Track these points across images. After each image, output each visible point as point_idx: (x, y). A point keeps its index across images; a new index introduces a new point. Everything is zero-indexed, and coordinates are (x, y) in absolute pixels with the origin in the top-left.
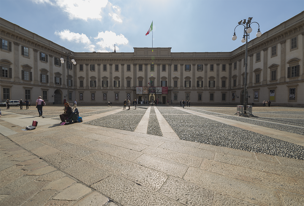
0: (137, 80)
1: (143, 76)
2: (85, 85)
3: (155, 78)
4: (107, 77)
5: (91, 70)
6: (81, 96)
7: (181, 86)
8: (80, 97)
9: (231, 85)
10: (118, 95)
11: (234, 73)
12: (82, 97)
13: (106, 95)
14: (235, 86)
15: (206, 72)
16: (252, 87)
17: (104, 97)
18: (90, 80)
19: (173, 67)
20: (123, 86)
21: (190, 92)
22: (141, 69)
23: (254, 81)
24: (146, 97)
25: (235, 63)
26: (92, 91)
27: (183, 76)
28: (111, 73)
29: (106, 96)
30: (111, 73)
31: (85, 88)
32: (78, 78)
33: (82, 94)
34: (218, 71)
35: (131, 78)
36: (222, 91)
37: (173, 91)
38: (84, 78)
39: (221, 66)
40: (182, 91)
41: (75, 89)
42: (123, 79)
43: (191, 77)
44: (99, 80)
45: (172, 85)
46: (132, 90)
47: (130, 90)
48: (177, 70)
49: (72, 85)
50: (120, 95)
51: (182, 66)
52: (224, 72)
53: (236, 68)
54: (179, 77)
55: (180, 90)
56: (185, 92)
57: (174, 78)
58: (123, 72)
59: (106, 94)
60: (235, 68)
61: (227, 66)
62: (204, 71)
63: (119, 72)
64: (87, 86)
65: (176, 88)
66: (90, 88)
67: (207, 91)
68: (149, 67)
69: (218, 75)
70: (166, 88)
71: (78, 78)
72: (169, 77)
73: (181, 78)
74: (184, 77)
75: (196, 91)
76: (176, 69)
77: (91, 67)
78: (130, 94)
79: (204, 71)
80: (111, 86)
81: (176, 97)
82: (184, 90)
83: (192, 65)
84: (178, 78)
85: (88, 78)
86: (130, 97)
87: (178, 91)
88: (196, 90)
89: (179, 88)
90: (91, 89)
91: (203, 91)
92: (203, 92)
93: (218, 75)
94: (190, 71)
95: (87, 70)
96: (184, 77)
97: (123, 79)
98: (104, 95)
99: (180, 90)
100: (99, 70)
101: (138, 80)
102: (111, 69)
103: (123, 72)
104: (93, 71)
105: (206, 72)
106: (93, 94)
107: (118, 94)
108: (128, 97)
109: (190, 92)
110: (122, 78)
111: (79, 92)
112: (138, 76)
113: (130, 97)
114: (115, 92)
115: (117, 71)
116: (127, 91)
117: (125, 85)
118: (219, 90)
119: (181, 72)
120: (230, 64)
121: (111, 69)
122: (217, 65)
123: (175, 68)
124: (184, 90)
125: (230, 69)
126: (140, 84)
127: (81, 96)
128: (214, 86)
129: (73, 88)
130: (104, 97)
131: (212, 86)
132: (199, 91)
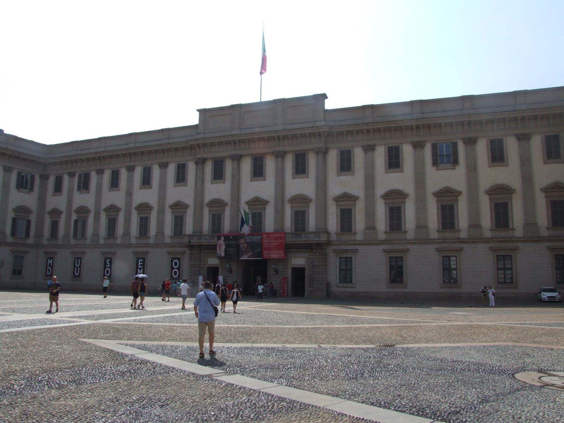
0: (206, 211)
2: (61, 232)
3: (267, 202)
5: (79, 189)
6: (50, 264)
7: (367, 228)
8: (47, 266)
10: (144, 262)
12: (52, 267)
15: (472, 169)
17: (105, 268)
18: (74, 217)
19: (333, 158)
21: (407, 251)
22: (218, 175)
24: (231, 271)
28: (129, 194)
29: (110, 267)
30: (129, 194)
31: (60, 242)
32: (49, 213)
33: (52, 258)
35: (186, 207)
36: (552, 244)
37: (335, 248)
41: (36, 246)
42: (161, 212)
45: (333, 224)
46: (191, 247)
49: (27, 235)
55: (363, 243)
56: (385, 251)
57: (339, 199)
59: (111, 259)
62: (461, 168)
64: (67, 235)
66: (73, 242)
67: (481, 245)
68: (247, 166)
70: (277, 238)
71: (49, 213)
73: (366, 196)
74: (380, 190)
78: (179, 259)
79: (461, 168)
82: (382, 242)
84: (354, 199)
86: (179, 268)
87: (357, 247)
88: (431, 241)
89: (359, 237)
91: (465, 246)
92: (461, 250)
95: (71, 191)
96: (380, 190)
97: (161, 212)
98: (105, 264)
99: (363, 243)
100: (99, 186)
101: (210, 211)
104: (84, 190)
105: (472, 169)
106: (78, 258)
107: (144, 259)
108: (172, 268)
109: (407, 251)
110: (159, 206)
111: (46, 253)
112: (207, 199)
113: (179, 268)
114: (135, 253)
115: (147, 186)
116: (171, 249)
117: (168, 230)
118: (537, 239)
121: (130, 181)
124: (382, 242)
127: (50, 264)
129: (30, 241)
130: (105, 268)
132: (445, 245)
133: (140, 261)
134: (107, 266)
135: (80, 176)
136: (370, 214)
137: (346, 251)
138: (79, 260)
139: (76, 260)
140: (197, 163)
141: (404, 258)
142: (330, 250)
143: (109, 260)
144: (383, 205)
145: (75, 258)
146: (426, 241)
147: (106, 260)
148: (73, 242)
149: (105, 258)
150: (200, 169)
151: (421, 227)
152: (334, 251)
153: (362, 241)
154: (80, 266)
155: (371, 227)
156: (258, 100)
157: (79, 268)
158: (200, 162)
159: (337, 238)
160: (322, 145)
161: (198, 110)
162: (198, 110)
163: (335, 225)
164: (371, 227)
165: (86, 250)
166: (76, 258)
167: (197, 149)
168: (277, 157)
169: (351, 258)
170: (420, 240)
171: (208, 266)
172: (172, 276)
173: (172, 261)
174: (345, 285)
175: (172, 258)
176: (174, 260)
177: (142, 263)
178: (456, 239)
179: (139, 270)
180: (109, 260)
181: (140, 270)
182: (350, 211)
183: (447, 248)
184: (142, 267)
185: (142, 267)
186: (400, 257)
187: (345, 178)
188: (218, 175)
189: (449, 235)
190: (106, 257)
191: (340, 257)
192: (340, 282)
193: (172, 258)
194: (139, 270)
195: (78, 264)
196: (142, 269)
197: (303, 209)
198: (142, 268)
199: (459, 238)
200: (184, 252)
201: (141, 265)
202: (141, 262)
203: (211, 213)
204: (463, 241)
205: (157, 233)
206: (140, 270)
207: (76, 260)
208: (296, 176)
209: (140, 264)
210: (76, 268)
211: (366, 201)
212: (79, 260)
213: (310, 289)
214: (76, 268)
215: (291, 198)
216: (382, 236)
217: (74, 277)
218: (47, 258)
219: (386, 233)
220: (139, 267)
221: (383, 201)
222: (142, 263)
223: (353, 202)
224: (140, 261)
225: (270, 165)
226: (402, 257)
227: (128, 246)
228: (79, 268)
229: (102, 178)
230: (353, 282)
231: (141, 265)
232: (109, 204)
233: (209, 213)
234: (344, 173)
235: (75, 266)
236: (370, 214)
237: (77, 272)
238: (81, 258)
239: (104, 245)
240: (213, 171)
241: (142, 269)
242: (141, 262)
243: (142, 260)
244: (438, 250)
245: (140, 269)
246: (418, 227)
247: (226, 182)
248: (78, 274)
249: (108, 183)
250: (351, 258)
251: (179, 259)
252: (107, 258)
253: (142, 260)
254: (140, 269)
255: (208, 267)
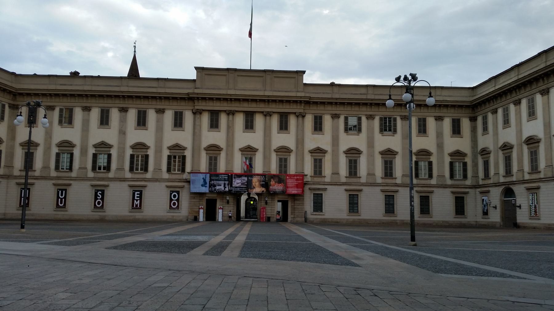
1: (222, 144)
2: (38, 163)
4: (109, 145)
9: (477, 173)
11: (485, 141)
13: (103, 194)
14: (488, 176)
16: (524, 182)
20: (158, 169)
21: (360, 191)
23: (527, 167)
25: (483, 117)
26: (60, 182)
27: (338, 145)
28: (122, 133)
29: (102, 199)
30: (122, 133)
34: (439, 135)
38: (37, 145)
39: (447, 123)
40: (337, 187)
43: (361, 149)
44: (84, 152)
45: (308, 169)
47: (180, 181)
48: (321, 129)
50: (147, 194)
51: (336, 120)
52: (457, 140)
53: (487, 130)
54: (326, 149)
56: (346, 190)
58: (160, 129)
60: (485, 129)
61: (466, 124)
63: (147, 130)
64: (46, 167)
65: (317, 180)
69: (440, 146)
72: (297, 148)
73: (333, 151)
75: (378, 189)
76: (318, 127)
77: (61, 116)
80: (120, 169)
81: (318, 206)
83: (364, 119)
85: (50, 145)
87: (326, 187)
90: (58, 178)
91: (399, 188)
93: (440, 146)
94: (360, 134)
97: (158, 151)
98: (96, 195)
102: (123, 121)
103: (160, 129)
106: (62, 190)
107: (141, 192)
108: (171, 200)
109: (360, 191)
110: (156, 146)
112: (205, 144)
119: (333, 136)
120: (473, 119)
121: (123, 121)
122: (436, 119)
123: (316, 123)
125: (474, 130)
126: (210, 164)
128: (431, 176)
130: (96, 199)
131: (425, 174)
133: (136, 193)
134: (98, 198)
135: (61, 111)
136: (335, 163)
137: (319, 189)
138: (64, 192)
139: (60, 191)
140: (194, 113)
141: (359, 196)
142: (307, 187)
143: (101, 193)
144: (345, 158)
145: (58, 189)
146: (374, 184)
147: (97, 192)
148: (54, 174)
149: (95, 190)
150: (198, 118)
151: (371, 174)
152: (310, 189)
153: (330, 182)
154: (65, 198)
155: (336, 173)
156: (248, 68)
157: (63, 199)
158: (197, 113)
159: (311, 179)
160: (302, 111)
161: (196, 68)
162: (196, 68)
163: (310, 170)
164: (336, 173)
165: (71, 182)
166: (60, 189)
167: (196, 101)
168: (265, 116)
169: (322, 194)
170: (371, 183)
171: (207, 198)
172: (170, 206)
173: (171, 194)
174: (317, 214)
175: (171, 191)
176: (172, 193)
177: (139, 196)
178: (394, 184)
179: (135, 200)
180: (101, 193)
181: (137, 202)
182: (321, 160)
183: (388, 190)
184: (139, 199)
185: (139, 199)
186: (356, 195)
187: (318, 137)
188: (214, 125)
189: (389, 181)
190: (97, 189)
191: (314, 194)
192: (314, 211)
193: (171, 191)
194: (135, 200)
195: (62, 195)
196: (139, 200)
197: (286, 157)
198: (138, 200)
199: (396, 184)
200: (182, 187)
201: (137, 197)
202: (137, 194)
203: (208, 155)
204: (397, 185)
205: (154, 169)
206: (137, 202)
207: (60, 191)
208: (282, 131)
209: (136, 195)
210: (60, 199)
211: (333, 154)
212: (64, 192)
213: (292, 216)
214: (60, 199)
215: (277, 148)
216: (344, 180)
217: (57, 207)
218: (21, 188)
219: (346, 177)
220: (136, 198)
221: (345, 155)
222: (139, 196)
223: (323, 154)
224: (136, 193)
225: (259, 121)
226: (358, 195)
227: (86, 179)
228: (63, 199)
229: (89, 115)
230: (323, 211)
231: (137, 197)
232: (98, 140)
233: (206, 156)
234: (316, 132)
235: (58, 197)
236: (335, 163)
237: (61, 203)
238: (66, 190)
239: (93, 178)
240: (210, 122)
241: (139, 200)
242: (137, 194)
243: (139, 193)
244: (382, 191)
245: (137, 200)
246: (369, 174)
247: (221, 131)
248: (62, 205)
249: (97, 121)
250: (322, 194)
251: (178, 193)
252: (98, 191)
253: (139, 193)
254: (137, 200)
255: (207, 199)
